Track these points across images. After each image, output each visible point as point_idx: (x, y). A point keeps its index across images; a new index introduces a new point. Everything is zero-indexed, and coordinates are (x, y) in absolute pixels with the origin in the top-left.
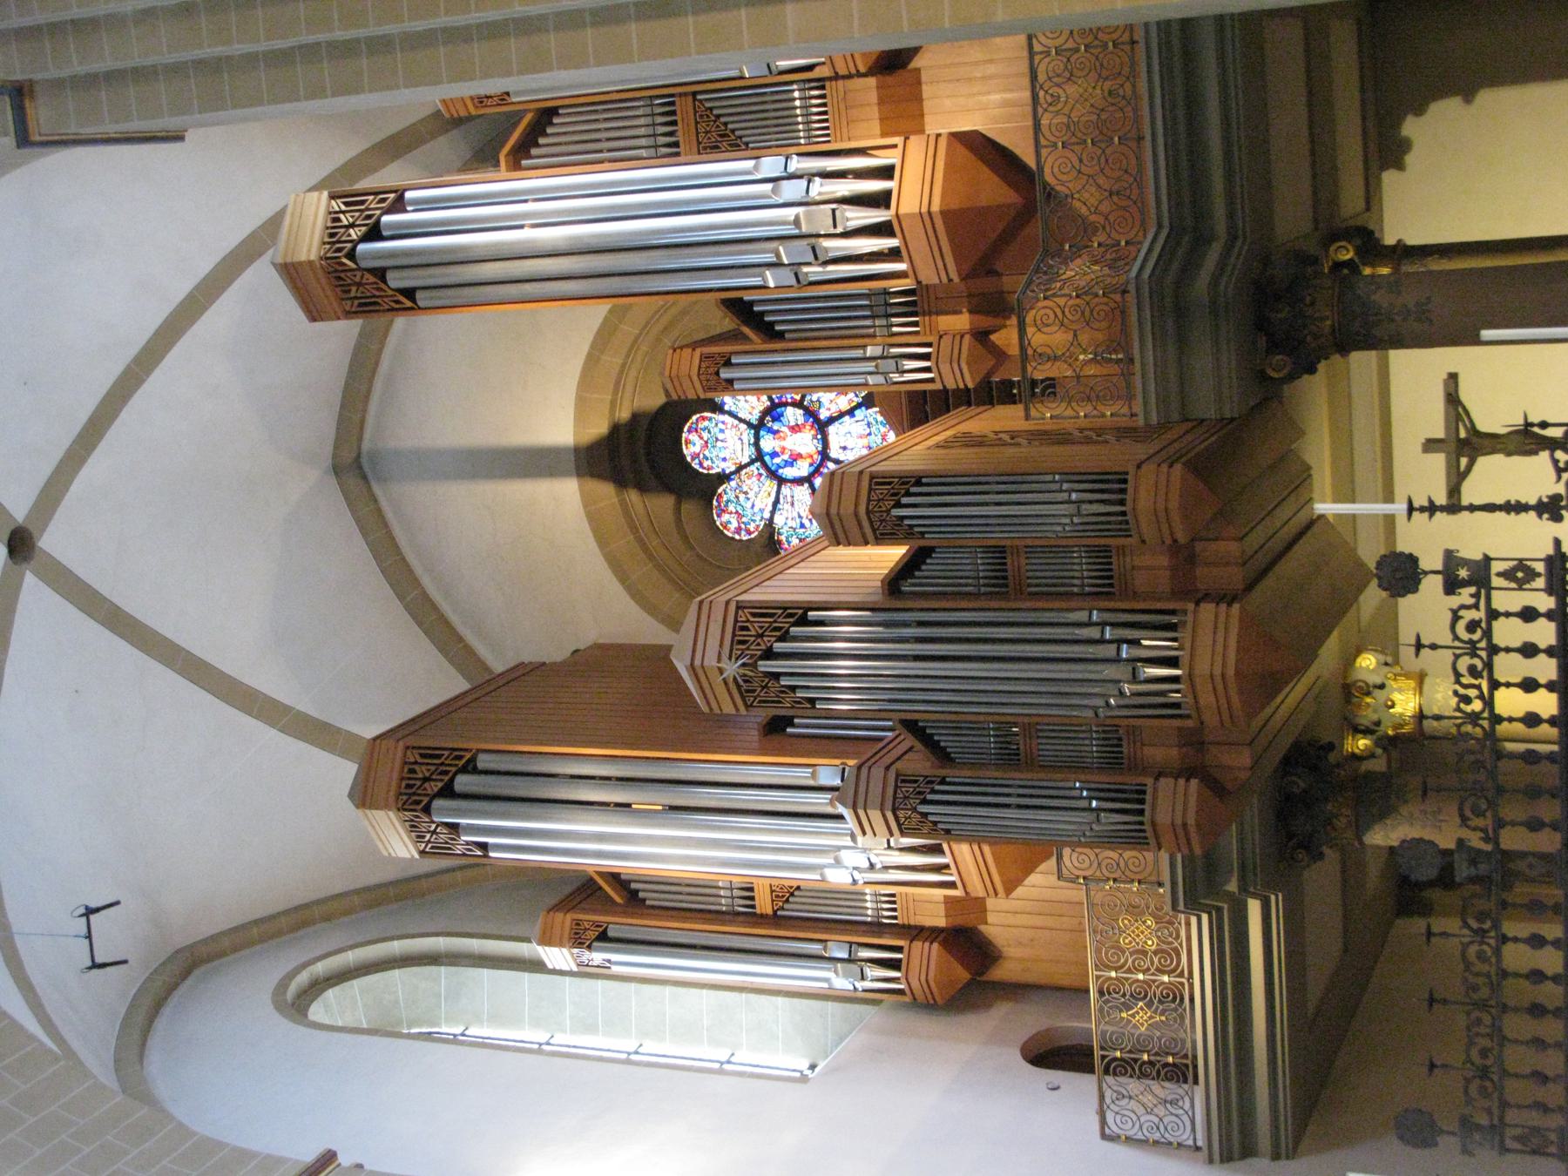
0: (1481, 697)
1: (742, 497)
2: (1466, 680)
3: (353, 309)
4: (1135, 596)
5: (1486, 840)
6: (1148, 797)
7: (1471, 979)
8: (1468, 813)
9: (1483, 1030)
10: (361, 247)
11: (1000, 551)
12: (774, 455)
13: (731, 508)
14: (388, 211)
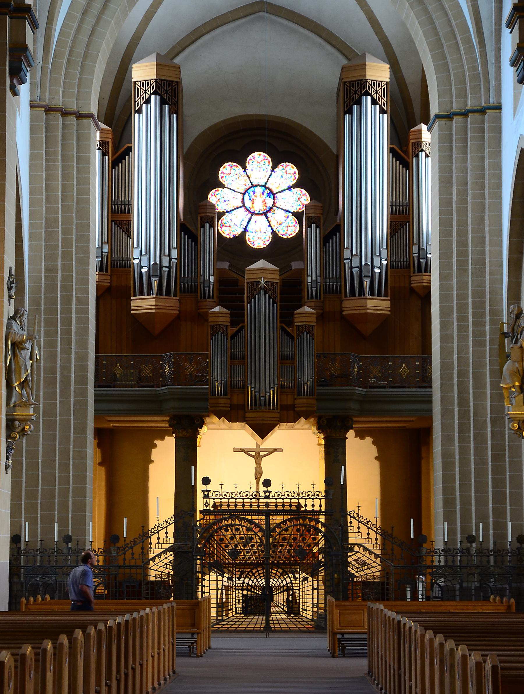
0: (303, 496)
1: (237, 177)
2: (307, 494)
3: (346, 86)
4: (280, 395)
5: (272, 497)
6: (225, 397)
7: (242, 493)
8: (278, 493)
9: (231, 495)
10: (369, 98)
11: (293, 358)
12: (254, 192)
13: (232, 171)
14: (380, 106)
